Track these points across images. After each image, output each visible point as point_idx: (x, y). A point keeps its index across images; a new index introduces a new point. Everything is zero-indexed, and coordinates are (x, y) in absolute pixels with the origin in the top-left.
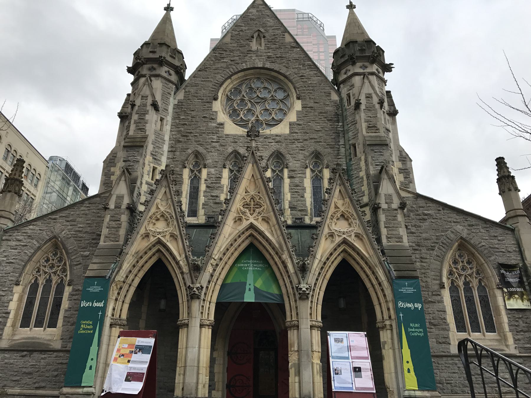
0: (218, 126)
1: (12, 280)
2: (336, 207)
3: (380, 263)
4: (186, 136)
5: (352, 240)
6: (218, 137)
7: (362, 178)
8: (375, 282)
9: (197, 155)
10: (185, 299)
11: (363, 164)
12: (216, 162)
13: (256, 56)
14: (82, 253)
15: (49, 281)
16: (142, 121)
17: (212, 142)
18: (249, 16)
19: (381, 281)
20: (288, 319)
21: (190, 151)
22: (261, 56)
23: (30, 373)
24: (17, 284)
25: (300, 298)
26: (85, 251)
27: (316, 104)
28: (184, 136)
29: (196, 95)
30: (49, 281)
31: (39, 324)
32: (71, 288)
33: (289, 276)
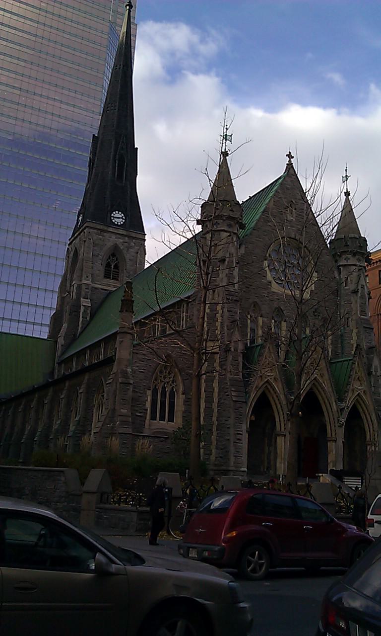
0: (268, 283)
1: (145, 386)
2: (356, 373)
3: (375, 410)
4: (248, 288)
5: (362, 394)
6: (268, 293)
7: (353, 345)
8: (369, 420)
9: (255, 304)
10: (282, 420)
11: (354, 335)
12: (268, 313)
13: (291, 226)
14: (188, 371)
15: (164, 388)
16: (231, 275)
17: (264, 296)
18: (285, 184)
19: (373, 419)
20: (329, 435)
21: (251, 301)
22: (293, 227)
23: (168, 453)
24: (149, 390)
25: (339, 426)
26: (190, 370)
27: (326, 279)
28: (247, 287)
29: (253, 252)
30: (164, 388)
31: (162, 418)
32: (184, 396)
33: (332, 412)
